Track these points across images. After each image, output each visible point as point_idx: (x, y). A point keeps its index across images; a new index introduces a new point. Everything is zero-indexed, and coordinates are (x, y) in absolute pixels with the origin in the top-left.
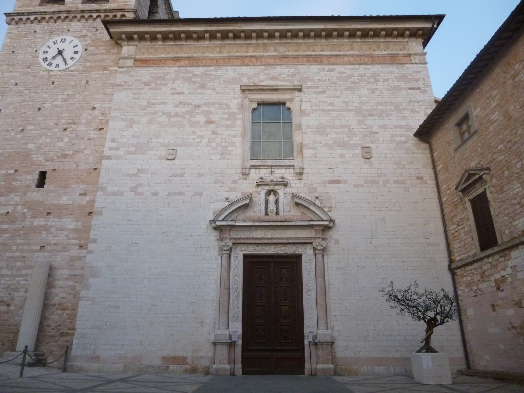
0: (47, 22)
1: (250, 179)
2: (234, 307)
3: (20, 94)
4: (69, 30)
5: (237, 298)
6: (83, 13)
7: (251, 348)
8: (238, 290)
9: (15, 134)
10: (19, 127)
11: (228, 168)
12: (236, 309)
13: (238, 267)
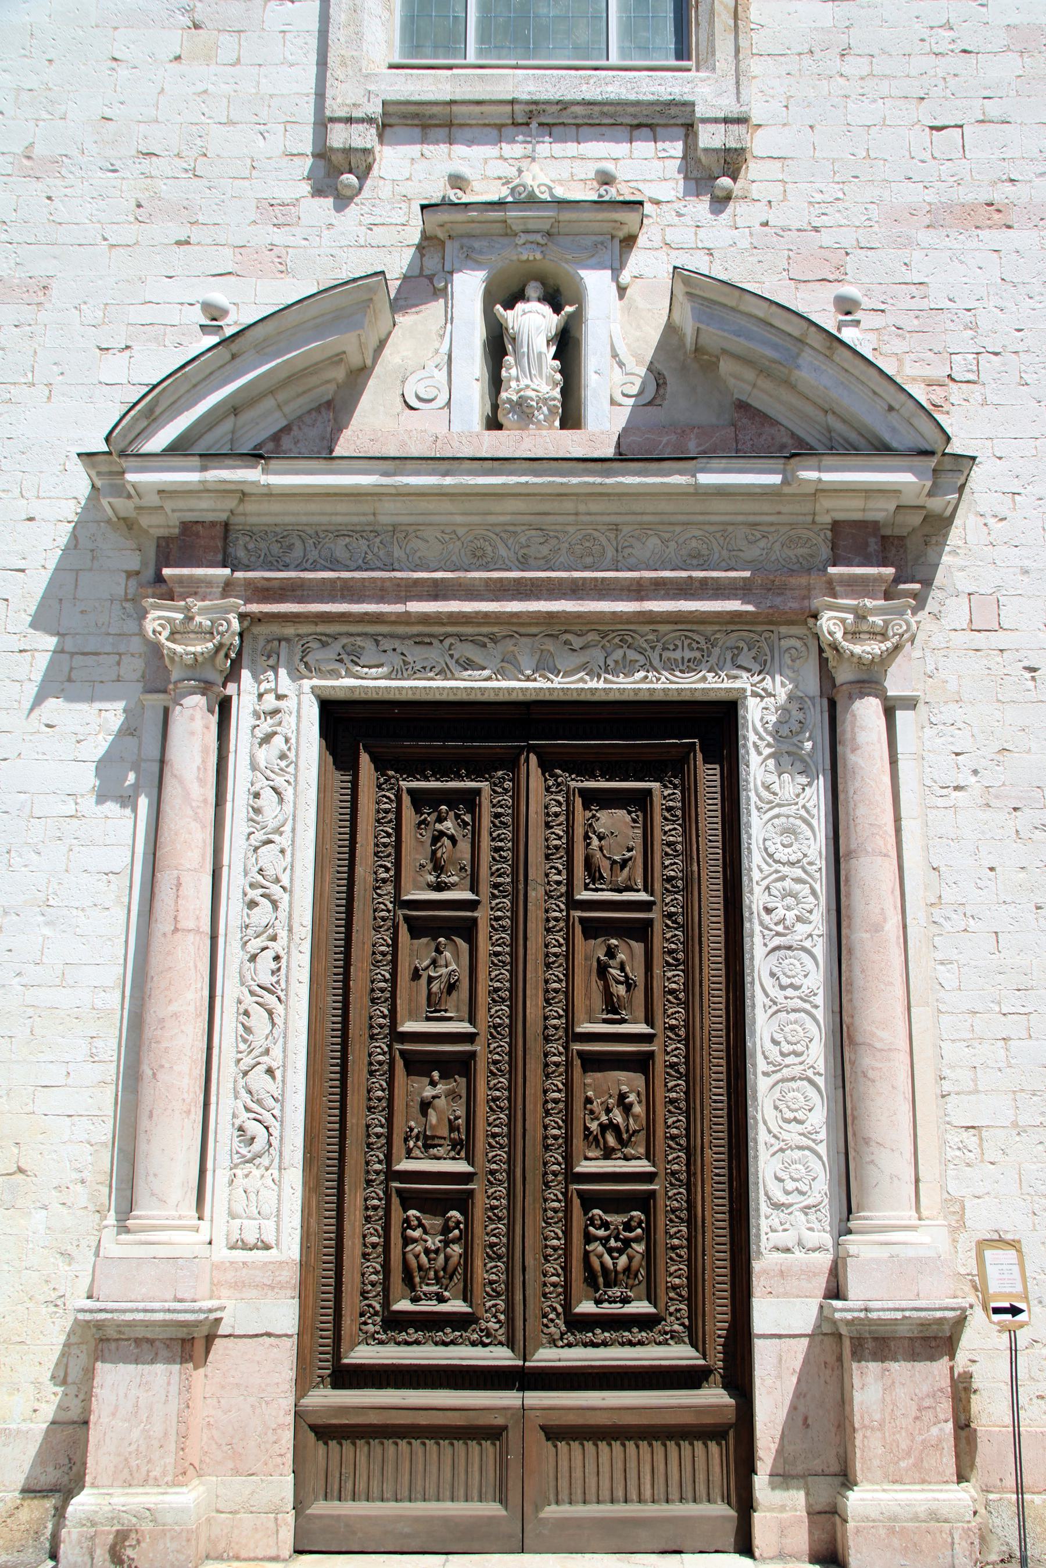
1: (385, 191)
2: (248, 1061)
5: (270, 999)
7: (364, 1354)
8: (277, 947)
11: (231, 123)
12: (259, 1080)
13: (279, 781)
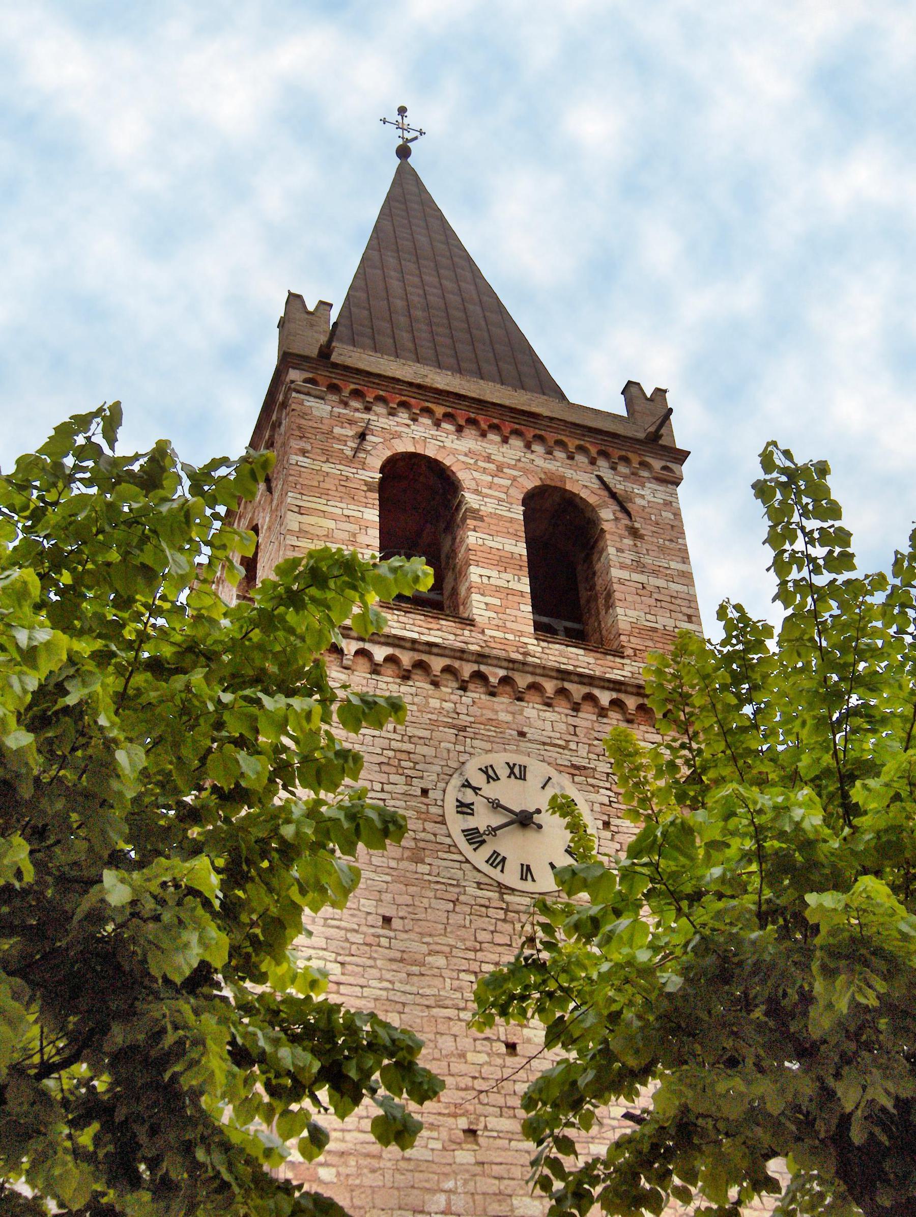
0: (435, 684)
3: (415, 969)
4: (522, 734)
6: (563, 680)
9: (444, 1149)
10: (455, 1116)
